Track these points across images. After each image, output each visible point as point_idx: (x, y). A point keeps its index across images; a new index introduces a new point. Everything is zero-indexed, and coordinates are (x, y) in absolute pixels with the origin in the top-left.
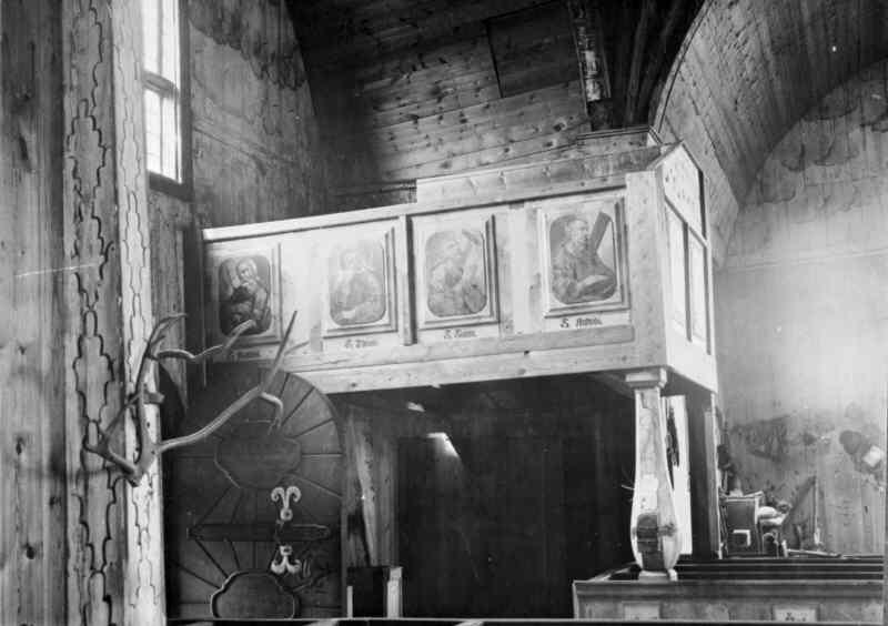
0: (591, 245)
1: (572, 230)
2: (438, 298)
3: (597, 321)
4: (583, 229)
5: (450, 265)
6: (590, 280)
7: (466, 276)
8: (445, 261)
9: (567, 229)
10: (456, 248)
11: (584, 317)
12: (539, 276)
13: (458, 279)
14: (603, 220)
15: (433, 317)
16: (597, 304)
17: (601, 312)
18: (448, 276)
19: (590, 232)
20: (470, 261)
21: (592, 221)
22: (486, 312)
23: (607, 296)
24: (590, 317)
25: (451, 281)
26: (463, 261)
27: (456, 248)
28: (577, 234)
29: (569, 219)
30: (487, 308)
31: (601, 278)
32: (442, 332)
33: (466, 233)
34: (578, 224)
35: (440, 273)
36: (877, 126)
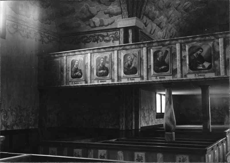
2: (126, 70)
4: (161, 54)
5: (129, 62)
6: (163, 67)
7: (133, 65)
8: (128, 61)
9: (158, 54)
10: (130, 58)
11: (161, 77)
13: (131, 66)
14: (167, 52)
15: (125, 75)
16: (165, 73)
17: (165, 75)
18: (129, 65)
20: (134, 61)
21: (164, 52)
22: (137, 74)
23: (166, 72)
25: (129, 66)
27: (130, 58)
28: (160, 55)
29: (159, 51)
30: (138, 73)
31: (165, 67)
32: (127, 79)
33: (133, 54)
34: (160, 53)
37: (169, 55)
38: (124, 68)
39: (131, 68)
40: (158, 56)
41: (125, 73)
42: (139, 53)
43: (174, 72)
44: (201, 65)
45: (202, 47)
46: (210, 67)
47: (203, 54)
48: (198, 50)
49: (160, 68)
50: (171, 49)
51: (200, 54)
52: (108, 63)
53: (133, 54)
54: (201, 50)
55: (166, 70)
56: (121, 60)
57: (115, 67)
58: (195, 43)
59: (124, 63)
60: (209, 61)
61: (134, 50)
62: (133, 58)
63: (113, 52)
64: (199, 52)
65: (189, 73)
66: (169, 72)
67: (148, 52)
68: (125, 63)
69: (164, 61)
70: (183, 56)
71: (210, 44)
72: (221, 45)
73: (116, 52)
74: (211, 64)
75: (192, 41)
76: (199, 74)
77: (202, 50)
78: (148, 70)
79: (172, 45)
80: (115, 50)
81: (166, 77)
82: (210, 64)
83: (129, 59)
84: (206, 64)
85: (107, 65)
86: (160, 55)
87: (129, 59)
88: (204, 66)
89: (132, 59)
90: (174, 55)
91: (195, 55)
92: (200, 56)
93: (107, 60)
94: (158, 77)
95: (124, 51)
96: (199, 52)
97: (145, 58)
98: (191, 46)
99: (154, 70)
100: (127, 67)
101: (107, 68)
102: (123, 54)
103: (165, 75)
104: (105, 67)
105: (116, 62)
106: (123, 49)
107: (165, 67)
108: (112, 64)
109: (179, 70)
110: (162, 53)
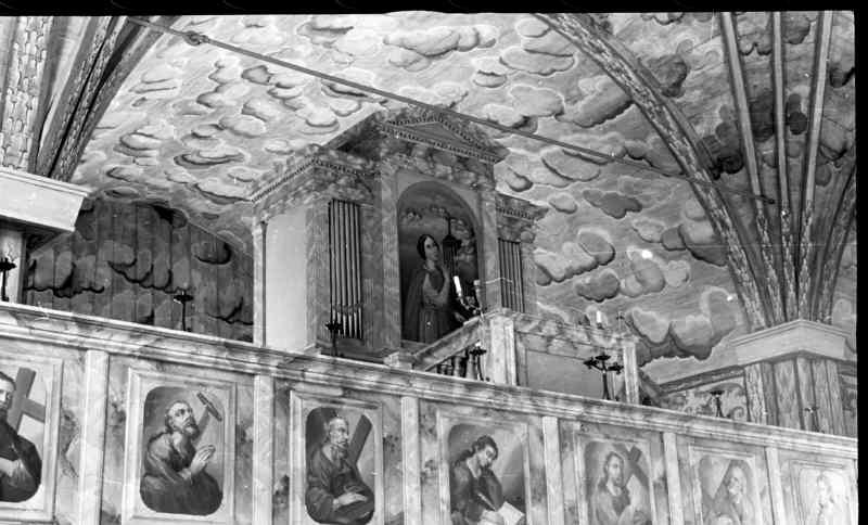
0: (352, 451)
1: (332, 426)
4: (343, 430)
5: (177, 438)
6: (348, 498)
7: (198, 461)
8: (170, 431)
9: (326, 427)
10: (187, 414)
12: (286, 480)
13: (187, 464)
18: (174, 452)
19: (350, 437)
21: (354, 421)
25: (177, 462)
26: (198, 433)
27: (187, 414)
29: (331, 414)
33: (201, 396)
34: (338, 422)
35: (162, 446)
37: (376, 438)
38: (149, 470)
39: (186, 474)
40: (328, 439)
41: (148, 498)
42: (234, 399)
45: (495, 438)
47: (499, 469)
49: (335, 501)
51: (489, 465)
52: (38, 413)
53: (201, 396)
54: (491, 449)
56: (122, 417)
57: (89, 452)
58: (467, 410)
59: (149, 441)
60: (519, 503)
61: (201, 373)
62: (198, 417)
63: (77, 354)
67: (281, 400)
68: (153, 439)
69: (354, 474)
70: (426, 459)
71: (521, 430)
72: (552, 443)
73: (95, 362)
74: (525, 518)
75: (462, 402)
77: (493, 445)
78: (280, 497)
80: (96, 348)
82: (522, 514)
83: (180, 421)
85: (28, 429)
86: (339, 430)
87: (180, 421)
89: (192, 423)
90: (391, 445)
91: (470, 463)
92: (486, 469)
93: (37, 395)
95: (143, 363)
96: (483, 456)
97: (260, 432)
98: (456, 422)
99: (308, 501)
100: (162, 468)
101: (33, 447)
102: (140, 382)
104: (18, 440)
105: (91, 421)
106: (143, 356)
107: (360, 498)
108: (69, 428)
110: (344, 426)
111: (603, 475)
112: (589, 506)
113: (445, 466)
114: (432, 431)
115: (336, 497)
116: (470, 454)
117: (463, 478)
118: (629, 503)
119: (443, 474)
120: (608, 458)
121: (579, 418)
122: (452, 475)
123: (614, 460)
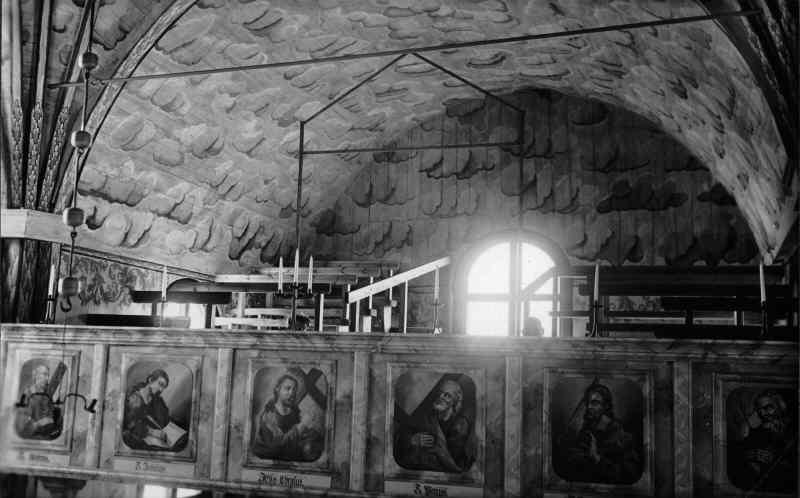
1: (37, 372)
3: (45, 459)
4: (45, 374)
16: (46, 443)
17: (49, 451)
21: (54, 367)
24: (42, 454)
34: (43, 369)
36: (431, 174)
43: (76, 444)
44: (156, 432)
45: (166, 370)
46: (182, 444)
47: (167, 396)
48: (154, 377)
50: (76, 359)
51: (159, 392)
54: (163, 380)
55: (52, 431)
60: (183, 422)
64: (155, 386)
65: (118, 454)
66: (60, 440)
74: (187, 434)
76: (150, 463)
77: (164, 375)
79: (82, 348)
81: (50, 456)
82: (184, 432)
84: (173, 433)
88: (164, 439)
91: (143, 392)
92: (156, 398)
94: (27, 455)
96: (155, 386)
103: (49, 451)
109: (91, 439)
111: (272, 396)
112: (253, 424)
113: (123, 395)
114: (117, 369)
115: (36, 420)
116: (144, 385)
117: (135, 402)
118: (299, 422)
119: (121, 402)
120: (280, 382)
121: (253, 347)
122: (127, 401)
123: (288, 383)
